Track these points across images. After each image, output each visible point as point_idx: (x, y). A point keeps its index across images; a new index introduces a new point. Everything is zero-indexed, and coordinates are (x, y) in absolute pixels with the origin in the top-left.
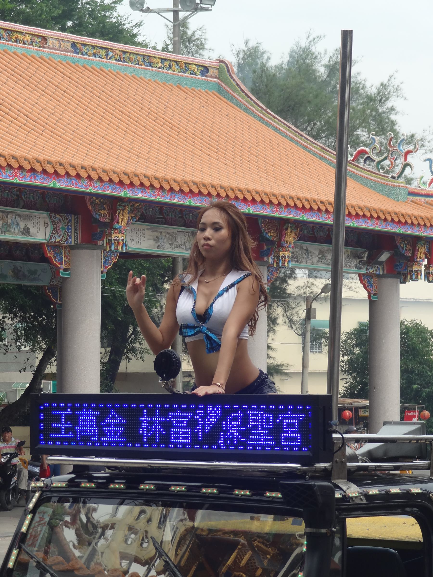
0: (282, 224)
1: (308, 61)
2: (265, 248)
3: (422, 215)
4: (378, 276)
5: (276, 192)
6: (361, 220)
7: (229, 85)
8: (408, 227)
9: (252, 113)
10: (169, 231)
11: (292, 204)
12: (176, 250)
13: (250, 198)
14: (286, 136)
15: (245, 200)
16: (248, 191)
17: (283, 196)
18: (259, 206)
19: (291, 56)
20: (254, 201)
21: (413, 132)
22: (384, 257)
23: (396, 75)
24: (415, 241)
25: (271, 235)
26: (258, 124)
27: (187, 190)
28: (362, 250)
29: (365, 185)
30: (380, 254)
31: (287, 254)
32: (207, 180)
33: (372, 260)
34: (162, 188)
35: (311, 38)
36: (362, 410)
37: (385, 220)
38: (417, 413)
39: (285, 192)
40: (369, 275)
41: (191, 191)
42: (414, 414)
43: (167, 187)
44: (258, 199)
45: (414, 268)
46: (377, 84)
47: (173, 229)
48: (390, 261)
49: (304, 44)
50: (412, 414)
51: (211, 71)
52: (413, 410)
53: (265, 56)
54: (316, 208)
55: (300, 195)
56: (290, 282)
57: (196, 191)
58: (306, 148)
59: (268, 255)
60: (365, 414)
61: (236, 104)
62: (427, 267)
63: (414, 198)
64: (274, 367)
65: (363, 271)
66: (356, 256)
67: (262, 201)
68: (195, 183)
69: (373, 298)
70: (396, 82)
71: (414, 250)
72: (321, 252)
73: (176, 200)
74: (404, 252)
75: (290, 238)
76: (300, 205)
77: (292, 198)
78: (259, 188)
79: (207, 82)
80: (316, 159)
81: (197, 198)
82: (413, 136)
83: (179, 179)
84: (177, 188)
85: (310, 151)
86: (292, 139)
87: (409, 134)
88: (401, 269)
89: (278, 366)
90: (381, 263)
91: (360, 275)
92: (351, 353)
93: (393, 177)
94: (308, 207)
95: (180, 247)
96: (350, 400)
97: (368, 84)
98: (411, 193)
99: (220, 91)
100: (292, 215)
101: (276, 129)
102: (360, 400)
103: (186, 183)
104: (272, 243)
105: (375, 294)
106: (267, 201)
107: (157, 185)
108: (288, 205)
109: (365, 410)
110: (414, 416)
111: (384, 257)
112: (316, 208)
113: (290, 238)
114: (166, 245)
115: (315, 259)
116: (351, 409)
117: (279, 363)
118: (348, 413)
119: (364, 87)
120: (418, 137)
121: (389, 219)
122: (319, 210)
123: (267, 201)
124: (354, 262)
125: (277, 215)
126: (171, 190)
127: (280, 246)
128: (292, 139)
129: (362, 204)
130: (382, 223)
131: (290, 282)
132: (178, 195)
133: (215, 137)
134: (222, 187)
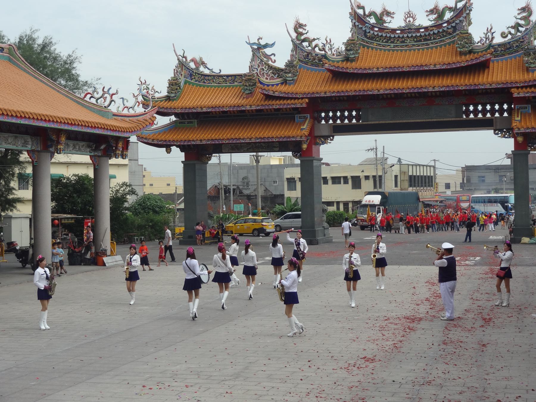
0: (59, 132)
1: (30, 42)
2: (49, 144)
3: (123, 126)
4: (99, 156)
5: (59, 116)
6: (97, 129)
7: (15, 57)
8: (117, 132)
9: (28, 73)
10: (6, 136)
11: (66, 122)
12: (8, 145)
13: (47, 119)
14: (47, 85)
15: (45, 120)
16: (47, 116)
17: (62, 118)
18: (51, 123)
19: (21, 39)
20: (49, 121)
21: (86, 80)
22: (102, 147)
23: (76, 51)
24: (117, 139)
25: (54, 137)
26: (33, 79)
27: (19, 115)
28: (92, 143)
29: (91, 110)
30: (101, 145)
31: (62, 147)
32: (28, 110)
33: (97, 149)
34: (7, 115)
35: (32, 30)
37: (107, 129)
39: (63, 116)
40: (95, 156)
41: (21, 116)
43: (10, 114)
44: (52, 120)
45: (117, 152)
46: (66, 55)
47: (6, 135)
48: (105, 148)
49: (28, 33)
51: (5, 50)
53: (6, 39)
54: (77, 124)
55: (70, 117)
56: (21, 155)
57: (23, 116)
58: (58, 91)
59: (51, 147)
61: (19, 68)
62: (122, 152)
63: (115, 117)
65: (92, 154)
66: (89, 146)
67: (53, 121)
68: (23, 112)
70: (78, 54)
71: (117, 144)
72: (74, 145)
73: (14, 121)
74: (112, 144)
75: (63, 139)
76: (70, 123)
77: (66, 119)
78: (52, 114)
79: (4, 56)
80: (65, 97)
81: (23, 119)
82: (86, 82)
83: (15, 110)
84: (15, 115)
85: (61, 93)
86: (51, 87)
87: (85, 81)
88: (109, 153)
90: (101, 150)
91: (90, 156)
93: (105, 107)
94: (73, 123)
95: (10, 144)
96: (56, 215)
97: (62, 55)
98: (114, 115)
99: (10, 60)
100: (66, 127)
101: (41, 81)
103: (18, 112)
104: (54, 141)
106: (55, 121)
107: (6, 114)
108: (65, 123)
110: (89, 222)
111: (102, 147)
112: (77, 124)
113: (63, 139)
114: (3, 143)
115: (71, 149)
116: (58, 219)
118: (57, 221)
119: (60, 56)
120: (89, 83)
121: (109, 128)
122: (78, 125)
123: (55, 121)
124: (88, 150)
125: (59, 127)
126: (12, 115)
127: (58, 143)
128: (51, 87)
129: (97, 121)
130: (106, 131)
131: (21, 155)
132: (15, 118)
133: (17, 86)
134: (35, 114)
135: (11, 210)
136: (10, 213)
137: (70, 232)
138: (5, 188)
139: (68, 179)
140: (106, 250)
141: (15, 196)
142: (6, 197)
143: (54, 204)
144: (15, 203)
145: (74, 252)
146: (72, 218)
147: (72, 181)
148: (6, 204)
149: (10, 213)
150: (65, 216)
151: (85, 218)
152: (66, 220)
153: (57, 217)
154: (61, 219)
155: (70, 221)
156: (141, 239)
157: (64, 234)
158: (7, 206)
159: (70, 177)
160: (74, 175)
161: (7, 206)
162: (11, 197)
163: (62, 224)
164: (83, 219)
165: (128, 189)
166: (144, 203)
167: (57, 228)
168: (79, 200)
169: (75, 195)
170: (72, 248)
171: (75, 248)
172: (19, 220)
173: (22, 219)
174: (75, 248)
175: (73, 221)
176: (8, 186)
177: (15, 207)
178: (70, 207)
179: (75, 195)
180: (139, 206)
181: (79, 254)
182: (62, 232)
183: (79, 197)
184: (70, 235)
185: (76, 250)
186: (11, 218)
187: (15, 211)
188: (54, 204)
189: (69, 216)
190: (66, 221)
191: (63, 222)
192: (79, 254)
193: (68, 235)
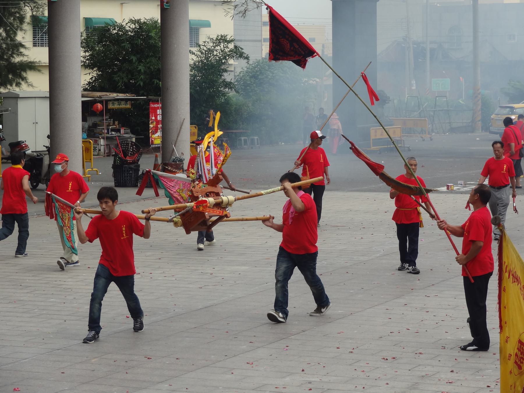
36: (111, 103)
38: (160, 105)
42: (158, 105)
50: (156, 106)
52: (157, 102)
60: (113, 107)
64: (28, 63)
69: (166, 6)
89: (30, 62)
92: (92, 49)
96: (98, 94)
102: (108, 94)
105: (167, 3)
109: (113, 103)
110: (158, 108)
116: (101, 102)
117: (32, 60)
118: (99, 106)
135: (18, 84)
136: (16, 90)
137: (123, 126)
138: (7, 44)
139: (121, 27)
140: (181, 161)
141: (25, 59)
142: (8, 60)
143: (94, 73)
144: (25, 71)
145: (123, 162)
146: (126, 100)
147: (127, 31)
148: (9, 72)
149: (16, 90)
150: (114, 95)
151: (150, 100)
152: (116, 103)
153: (100, 97)
154: (107, 101)
155: (123, 106)
156: (253, 140)
157: (112, 130)
158: (10, 76)
159: (124, 24)
160: (132, 21)
161: (10, 76)
162: (17, 59)
163: (108, 111)
164: (147, 102)
165: (231, 46)
166: (261, 73)
167: (100, 118)
168: (141, 68)
169: (134, 59)
170: (121, 155)
171: (125, 155)
172: (31, 102)
173: (38, 101)
174: (125, 155)
175: (128, 106)
176: (13, 40)
177: (24, 79)
178: (125, 80)
179: (134, 59)
180: (253, 80)
181: (132, 166)
182: (109, 125)
183: (140, 61)
184: (122, 131)
185: (128, 159)
186: (16, 97)
187: (24, 85)
188: (94, 73)
189: (121, 96)
190: (116, 106)
191: (110, 106)
192: (132, 166)
193: (118, 131)
